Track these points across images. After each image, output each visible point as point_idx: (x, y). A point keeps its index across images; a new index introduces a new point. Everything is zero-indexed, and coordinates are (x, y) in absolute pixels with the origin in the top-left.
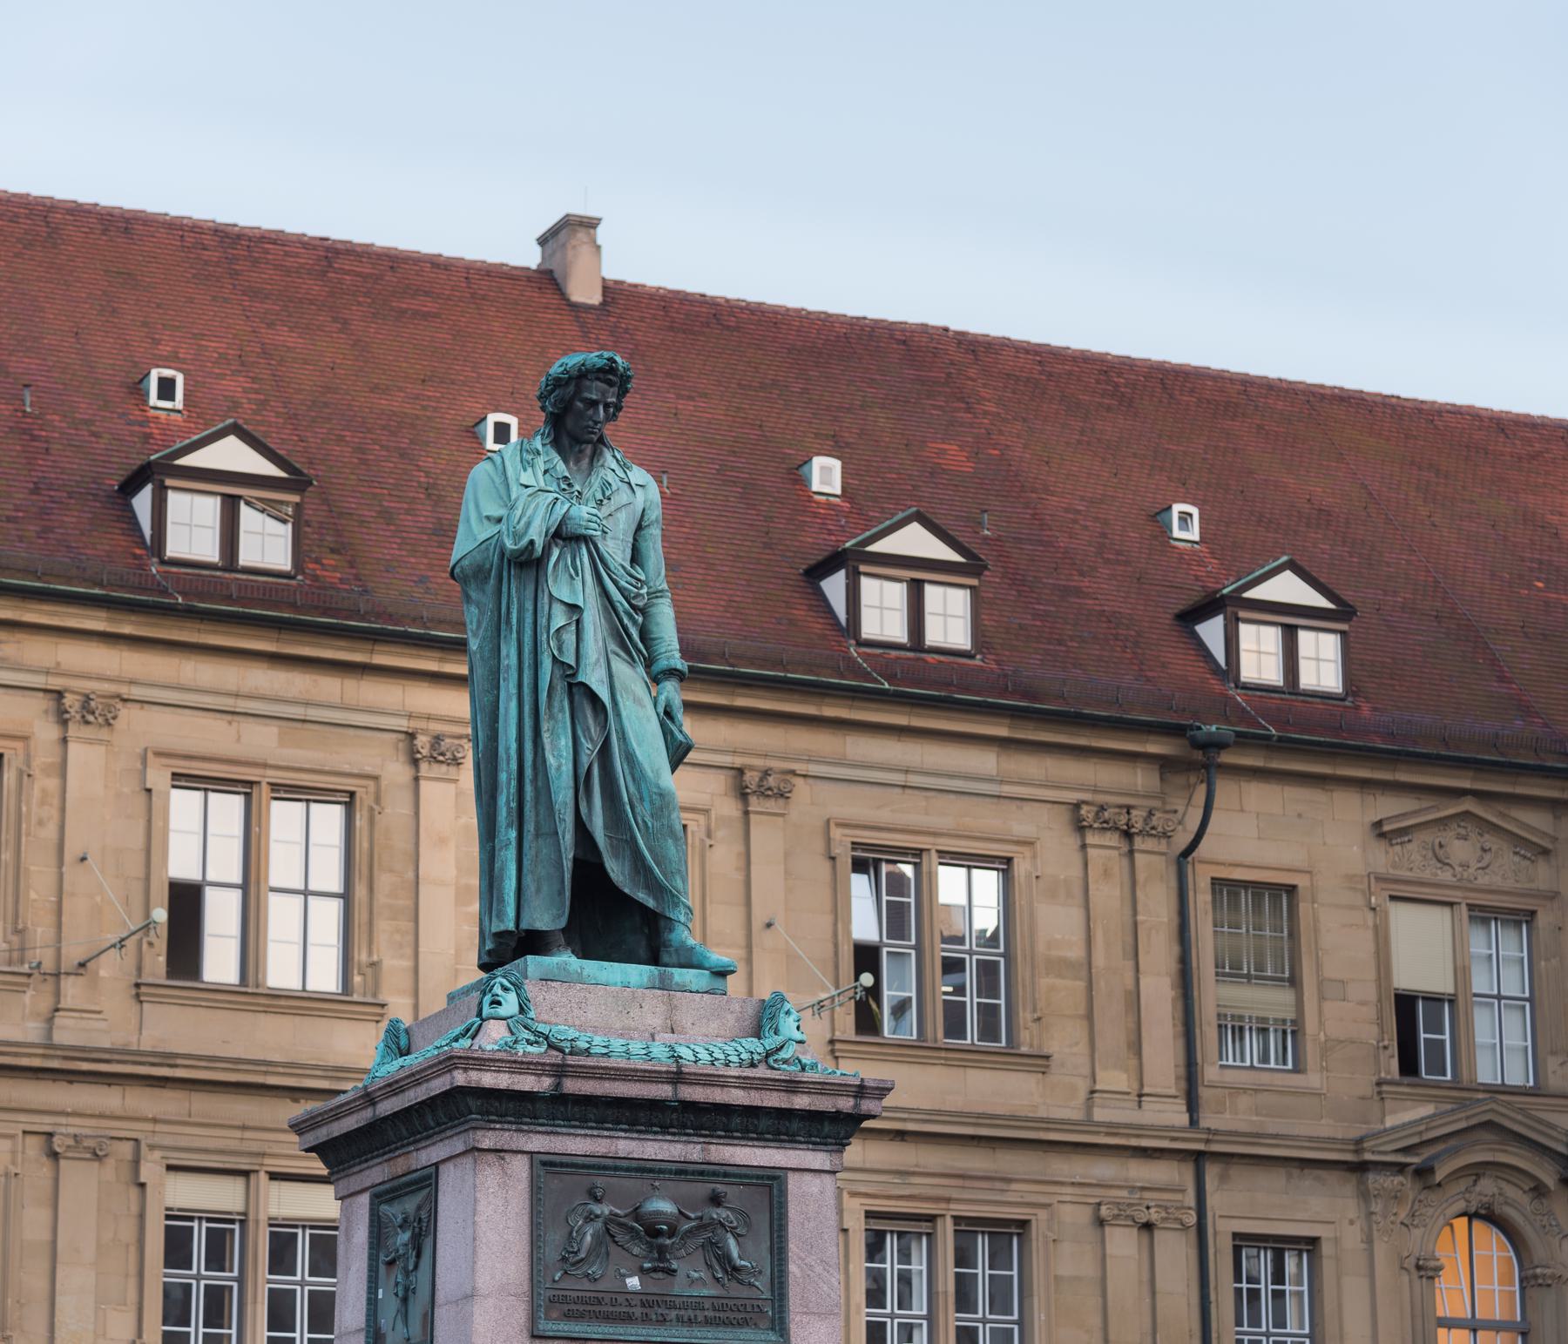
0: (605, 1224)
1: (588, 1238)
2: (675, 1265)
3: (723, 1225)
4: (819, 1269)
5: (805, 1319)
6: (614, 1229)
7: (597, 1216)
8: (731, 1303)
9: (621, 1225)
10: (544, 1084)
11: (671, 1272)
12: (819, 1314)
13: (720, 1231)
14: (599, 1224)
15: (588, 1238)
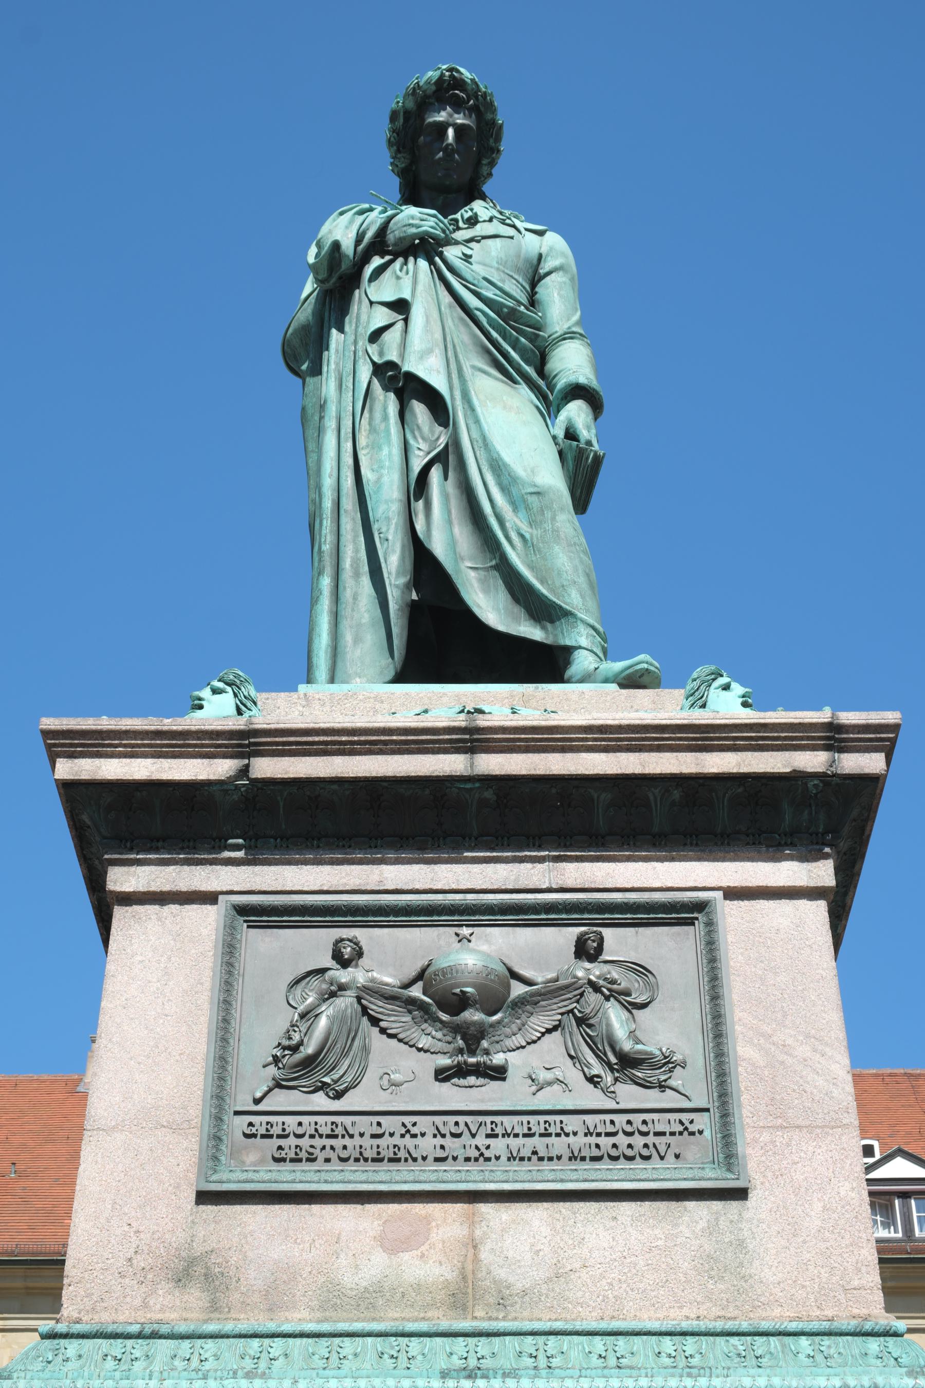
0: (359, 999)
1: (181, 856)
2: (498, 1059)
3: (596, 988)
4: (803, 1051)
5: (781, 1138)
6: (376, 1007)
7: (342, 987)
8: (620, 1119)
9: (391, 998)
10: (221, 769)
11: (499, 1073)
12: (810, 1128)
13: (592, 998)
14: (346, 1002)
15: (181, 856)
